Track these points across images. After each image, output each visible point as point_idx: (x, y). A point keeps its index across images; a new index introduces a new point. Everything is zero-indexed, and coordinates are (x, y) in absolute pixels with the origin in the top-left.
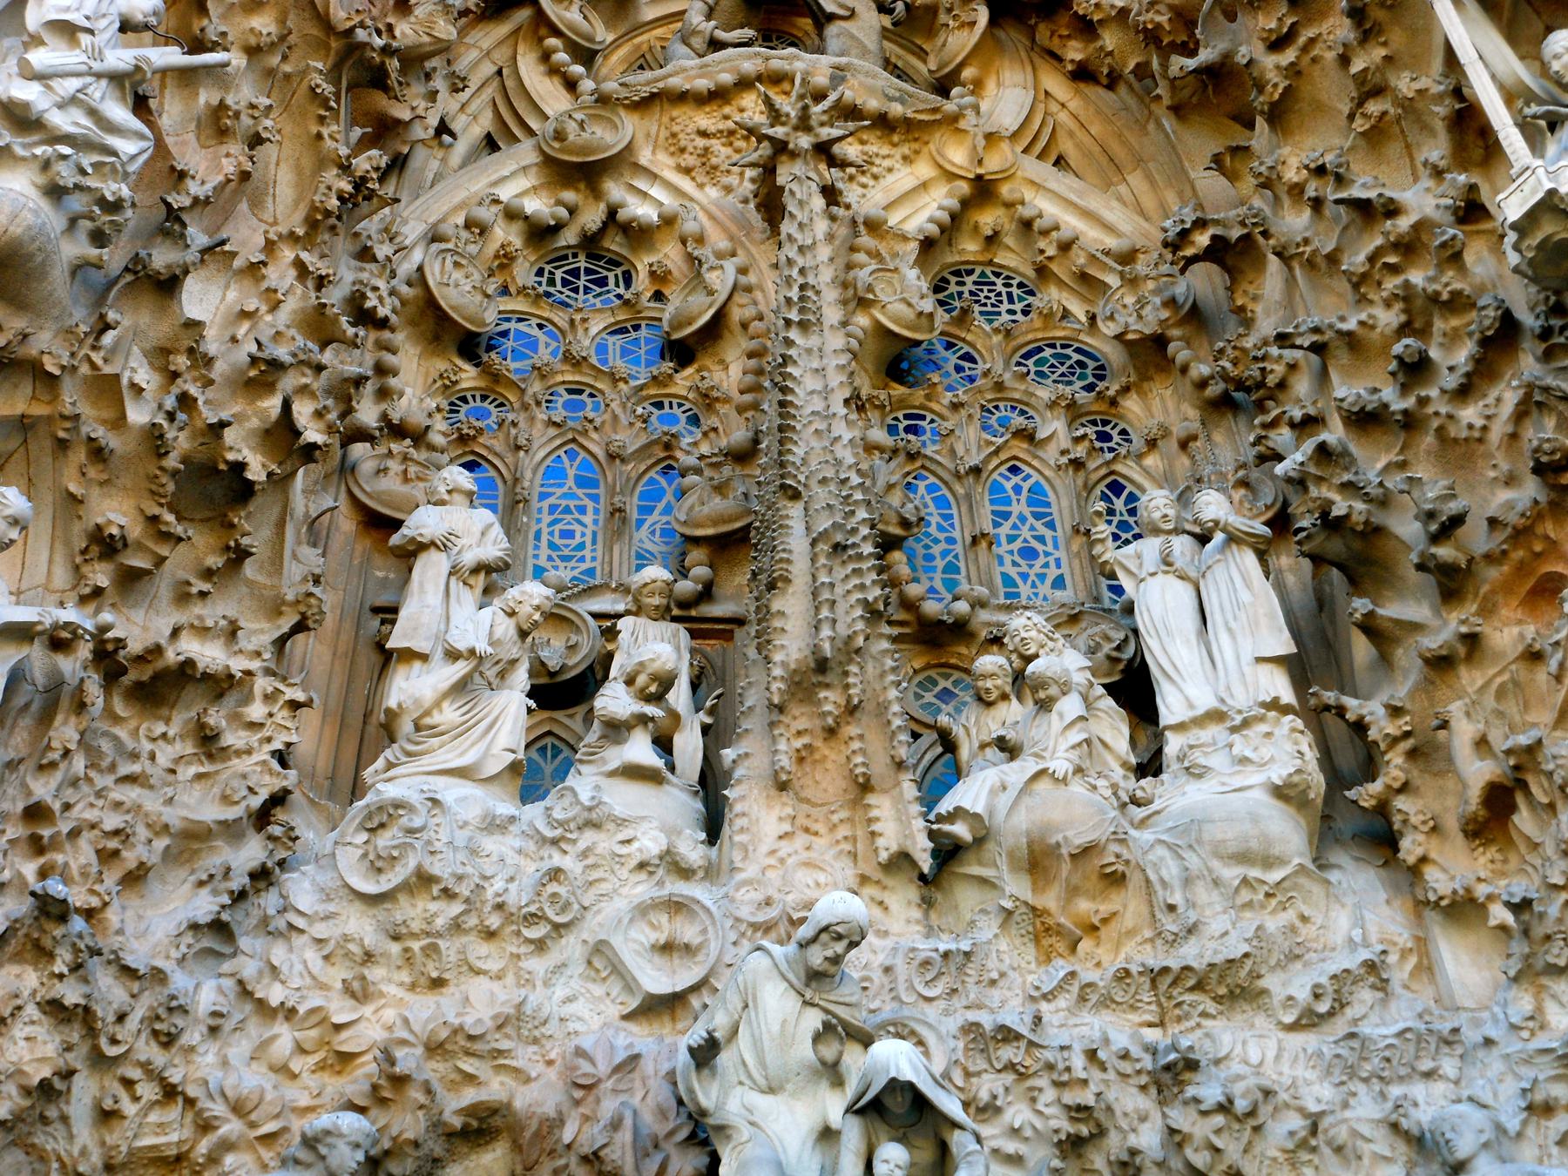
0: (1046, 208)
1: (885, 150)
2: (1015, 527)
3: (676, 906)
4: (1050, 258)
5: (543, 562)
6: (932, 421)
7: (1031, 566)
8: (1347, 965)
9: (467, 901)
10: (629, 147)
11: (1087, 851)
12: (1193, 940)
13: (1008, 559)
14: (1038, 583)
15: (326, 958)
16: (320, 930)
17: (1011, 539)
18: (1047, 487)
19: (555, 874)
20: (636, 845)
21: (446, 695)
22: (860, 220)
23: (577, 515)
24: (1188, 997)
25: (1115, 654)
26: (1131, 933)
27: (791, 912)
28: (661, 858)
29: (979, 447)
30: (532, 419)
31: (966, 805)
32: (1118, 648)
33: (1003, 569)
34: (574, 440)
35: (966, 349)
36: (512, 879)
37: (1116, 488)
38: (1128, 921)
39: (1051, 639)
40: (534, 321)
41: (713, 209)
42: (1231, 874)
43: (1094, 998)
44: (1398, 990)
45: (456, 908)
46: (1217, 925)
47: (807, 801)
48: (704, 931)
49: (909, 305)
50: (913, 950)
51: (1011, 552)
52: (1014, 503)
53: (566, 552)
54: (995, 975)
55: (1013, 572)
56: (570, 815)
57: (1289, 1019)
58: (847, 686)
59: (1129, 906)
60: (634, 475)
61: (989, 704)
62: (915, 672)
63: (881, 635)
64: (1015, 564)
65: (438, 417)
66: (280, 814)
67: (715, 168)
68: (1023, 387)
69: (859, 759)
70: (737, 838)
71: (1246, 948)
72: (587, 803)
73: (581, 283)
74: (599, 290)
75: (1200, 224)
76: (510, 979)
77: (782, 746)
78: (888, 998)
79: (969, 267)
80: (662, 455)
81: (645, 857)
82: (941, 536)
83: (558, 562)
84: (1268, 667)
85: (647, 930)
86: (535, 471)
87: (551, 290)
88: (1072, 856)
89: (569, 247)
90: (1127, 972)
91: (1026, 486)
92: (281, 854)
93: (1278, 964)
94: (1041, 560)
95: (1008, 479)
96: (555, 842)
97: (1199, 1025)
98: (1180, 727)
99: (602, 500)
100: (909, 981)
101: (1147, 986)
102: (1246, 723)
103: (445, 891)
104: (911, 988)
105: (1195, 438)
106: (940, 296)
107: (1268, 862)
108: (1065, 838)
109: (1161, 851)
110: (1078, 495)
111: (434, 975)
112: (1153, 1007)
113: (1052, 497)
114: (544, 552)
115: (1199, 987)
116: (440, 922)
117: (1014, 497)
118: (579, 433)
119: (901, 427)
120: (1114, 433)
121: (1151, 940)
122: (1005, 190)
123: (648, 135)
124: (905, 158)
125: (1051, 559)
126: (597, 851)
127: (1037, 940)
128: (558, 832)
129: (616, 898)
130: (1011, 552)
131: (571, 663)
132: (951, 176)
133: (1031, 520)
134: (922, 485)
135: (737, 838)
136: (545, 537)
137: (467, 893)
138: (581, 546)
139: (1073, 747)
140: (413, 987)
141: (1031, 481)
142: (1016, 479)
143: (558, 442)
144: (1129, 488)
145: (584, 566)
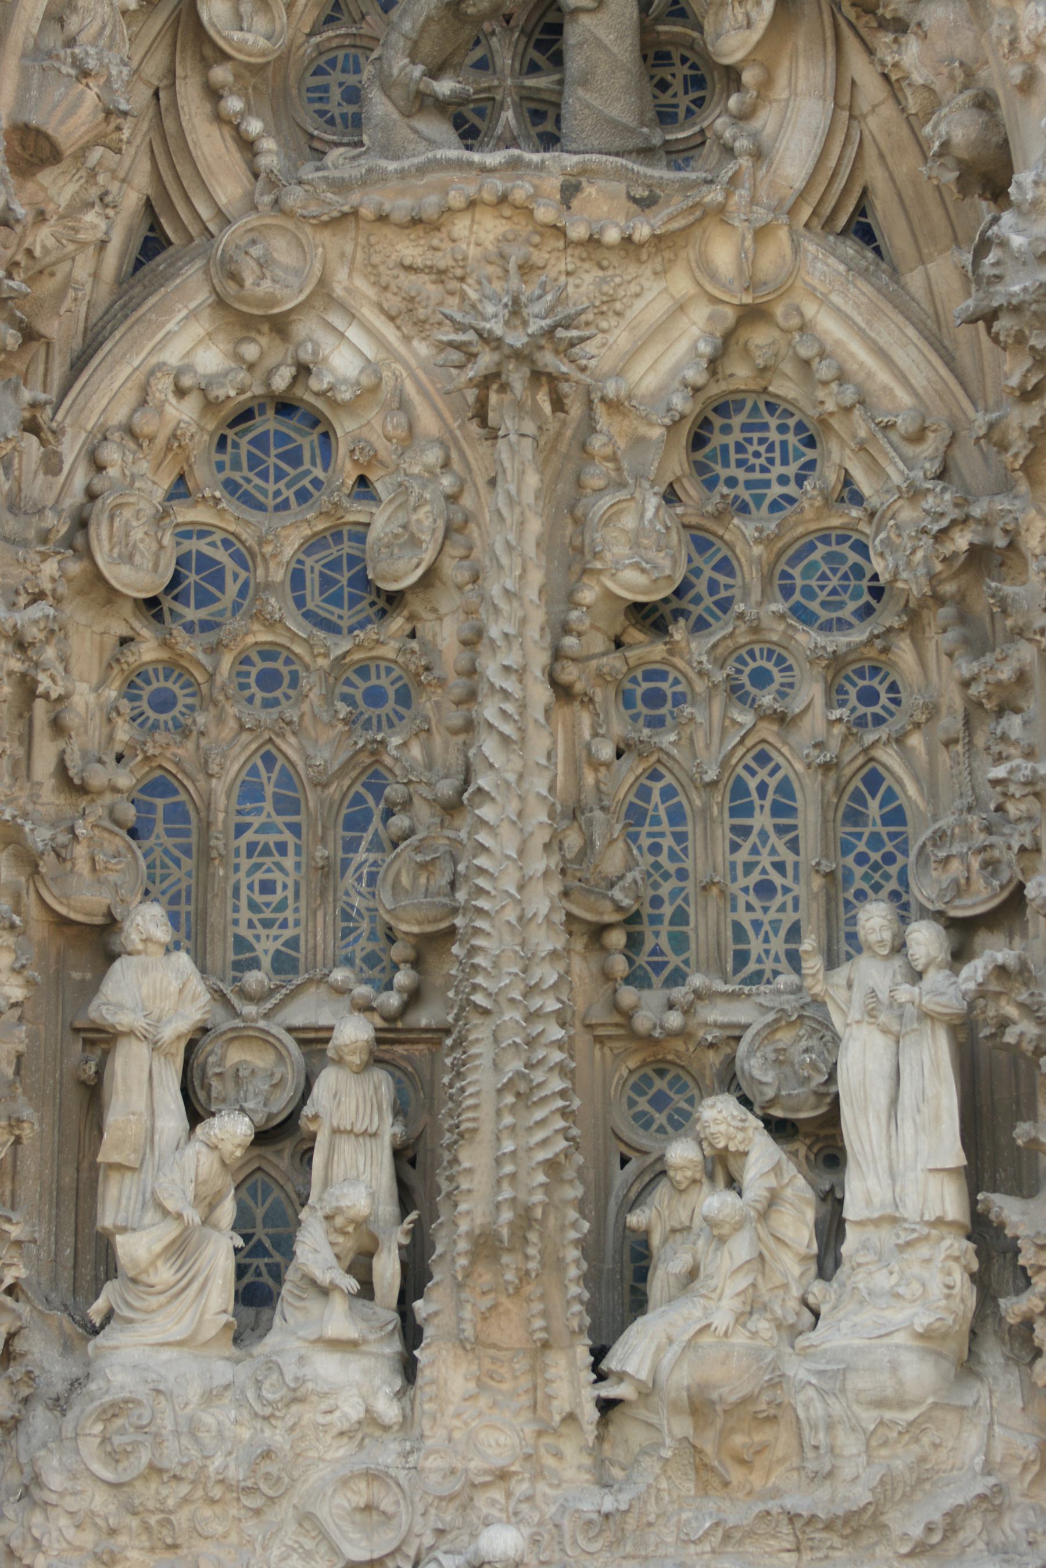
0: (829, 326)
1: (632, 270)
2: (754, 850)
3: (373, 1476)
4: (831, 414)
5: (243, 930)
6: (676, 682)
7: (765, 909)
8: (961, 1501)
9: (193, 1482)
10: (323, 282)
11: (744, 1401)
12: (828, 1483)
13: (742, 899)
14: (771, 934)
15: (78, 1527)
16: (71, 1503)
17: (749, 867)
18: (796, 785)
19: (267, 1454)
20: (337, 1414)
21: (158, 1256)
22: (596, 397)
23: (277, 858)
24: (817, 1535)
25: (823, 1089)
26: (782, 1461)
27: (472, 1476)
28: (359, 1423)
29: (724, 730)
30: (220, 720)
31: (630, 1369)
32: (826, 1083)
33: (735, 916)
34: (270, 740)
35: (725, 551)
36: (230, 1453)
37: (873, 780)
38: (779, 1453)
39: (743, 1129)
40: (218, 537)
41: (423, 377)
42: (868, 1418)
43: (737, 1535)
44: (1017, 1499)
45: (184, 1489)
46: (847, 1471)
47: (494, 1346)
48: (397, 1503)
49: (643, 571)
50: (577, 1511)
51: (746, 890)
52: (757, 810)
53: (267, 914)
54: (652, 1518)
55: (745, 919)
56: (277, 1396)
57: (904, 1550)
58: (527, 1257)
59: (783, 1440)
60: (337, 797)
61: (681, 1192)
62: (631, 1072)
63: (562, 1181)
64: (749, 908)
65: (120, 721)
66: (19, 1345)
67: (424, 322)
68: (781, 627)
69: (539, 1323)
70: (427, 1407)
71: (868, 1497)
72: (292, 1385)
73: (272, 461)
74: (292, 472)
75: (965, 520)
76: (234, 1538)
77: (467, 1313)
78: (556, 1548)
79: (740, 397)
80: (368, 761)
81: (346, 1426)
82: (671, 867)
83: (260, 930)
84: (939, 1176)
85: (349, 1495)
86: (229, 795)
87: (237, 476)
88: (725, 1411)
89: (254, 397)
90: (768, 1513)
91: (773, 783)
92: (25, 1391)
93: (904, 1495)
94: (779, 899)
95: (753, 773)
96: (266, 1418)
97: (827, 1557)
98: (860, 1223)
99: (304, 831)
100: (574, 1537)
101: (786, 1521)
102: (909, 1244)
103: (175, 1477)
104: (575, 1542)
105: (956, 741)
106: (699, 455)
107: (902, 1405)
108: (721, 1397)
109: (811, 1392)
110: (824, 807)
111: (169, 1541)
112: (791, 1538)
113: (799, 804)
114: (245, 914)
115: (828, 1527)
116: (171, 1503)
117: (757, 803)
118: (277, 735)
119: (639, 692)
120: (882, 690)
121: (798, 1469)
122: (779, 311)
123: (343, 255)
124: (656, 273)
125: (789, 898)
126: (304, 1422)
127: (697, 1470)
128: (268, 1411)
129: (321, 1465)
130: (746, 890)
131: (275, 1110)
132: (714, 300)
133: (773, 838)
134: (657, 787)
135: (427, 1407)
136: (244, 892)
137: (191, 1477)
138: (282, 906)
139: (738, 1294)
140: (152, 1549)
141: (779, 775)
142: (762, 774)
143: (254, 746)
144: (889, 781)
145: (288, 934)
